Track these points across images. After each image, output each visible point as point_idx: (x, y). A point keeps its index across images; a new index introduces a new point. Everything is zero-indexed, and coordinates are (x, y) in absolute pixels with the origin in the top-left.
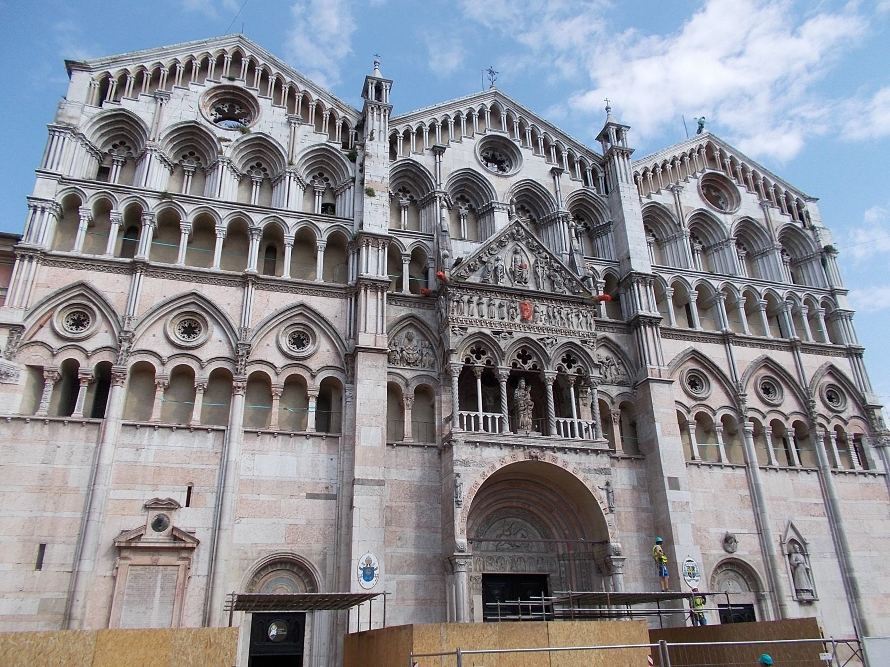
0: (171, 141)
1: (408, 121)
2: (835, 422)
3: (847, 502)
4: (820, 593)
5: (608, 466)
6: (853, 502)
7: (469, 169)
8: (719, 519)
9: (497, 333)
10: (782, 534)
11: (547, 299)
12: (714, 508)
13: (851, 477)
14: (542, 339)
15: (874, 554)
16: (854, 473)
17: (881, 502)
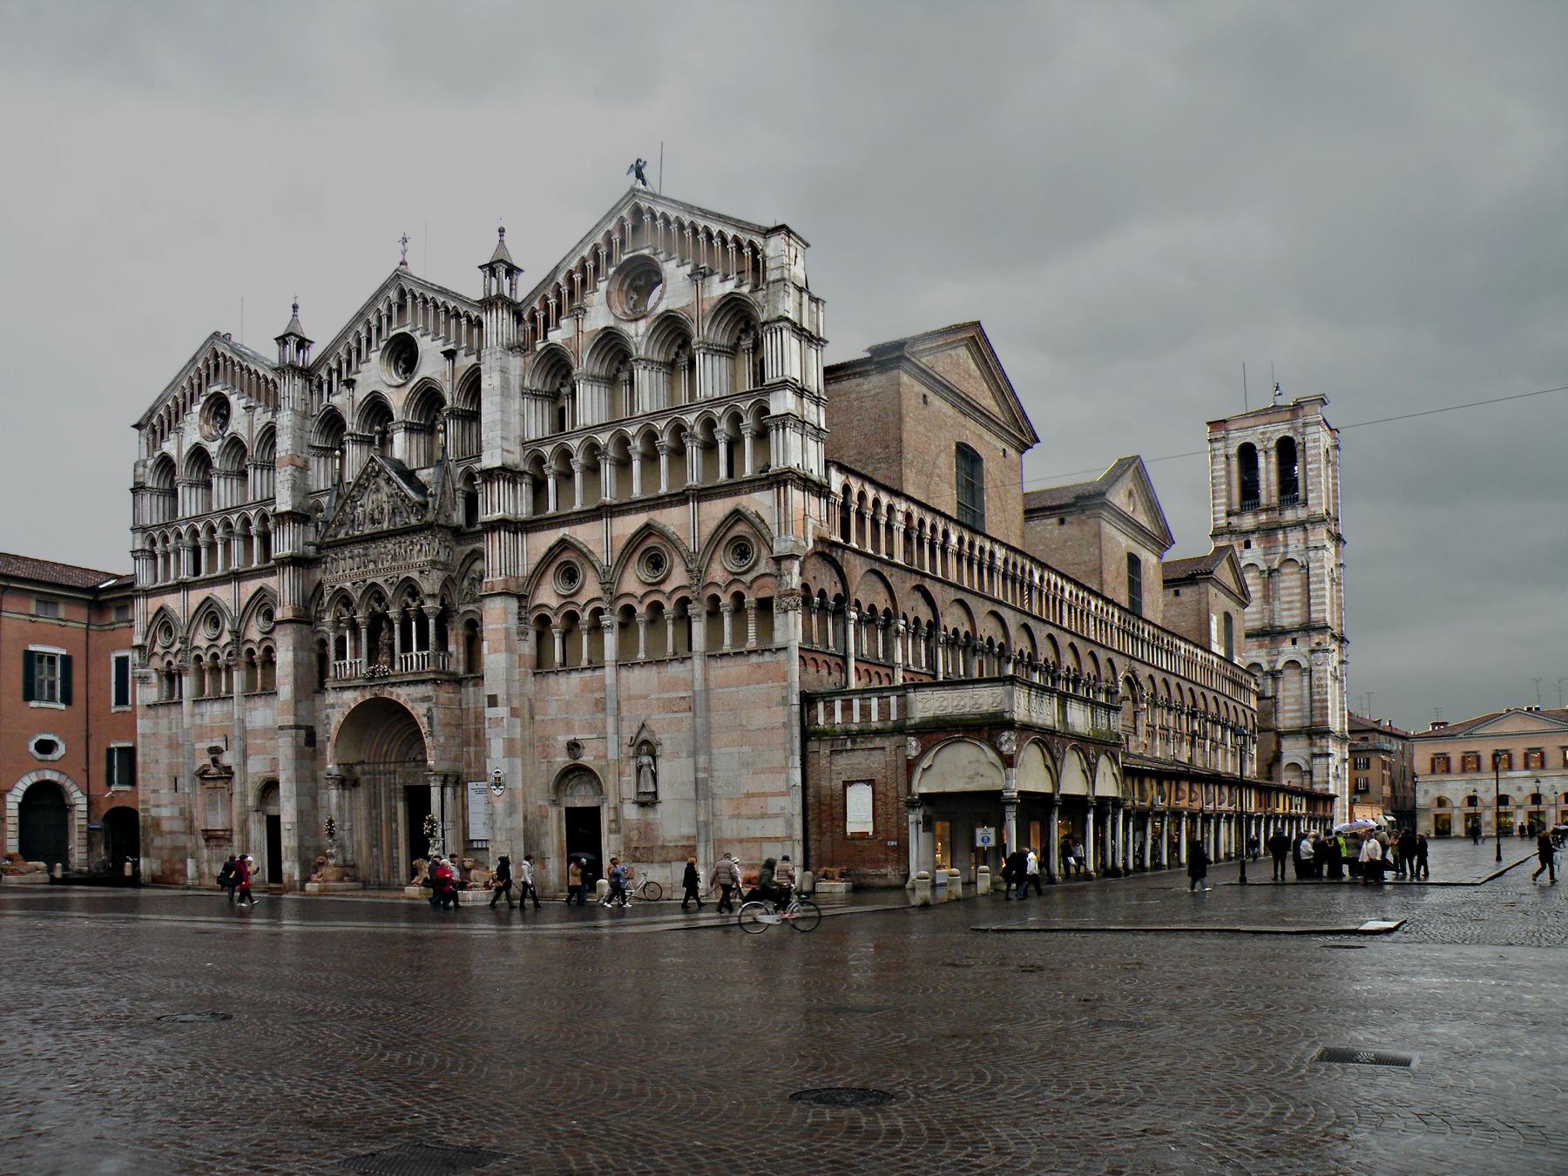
0: (194, 464)
1: (328, 359)
2: (734, 588)
3: (726, 690)
4: (661, 796)
5: (431, 694)
6: (734, 689)
7: (373, 392)
8: (569, 726)
9: (354, 584)
10: (634, 736)
11: (392, 536)
12: (564, 716)
13: (740, 660)
14: (387, 580)
15: (745, 749)
16: (742, 653)
17: (776, 684)
